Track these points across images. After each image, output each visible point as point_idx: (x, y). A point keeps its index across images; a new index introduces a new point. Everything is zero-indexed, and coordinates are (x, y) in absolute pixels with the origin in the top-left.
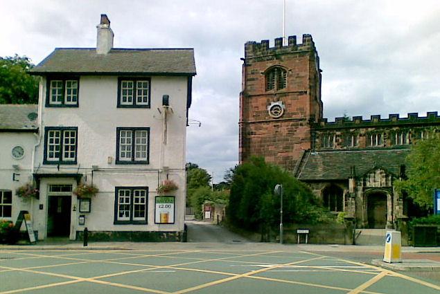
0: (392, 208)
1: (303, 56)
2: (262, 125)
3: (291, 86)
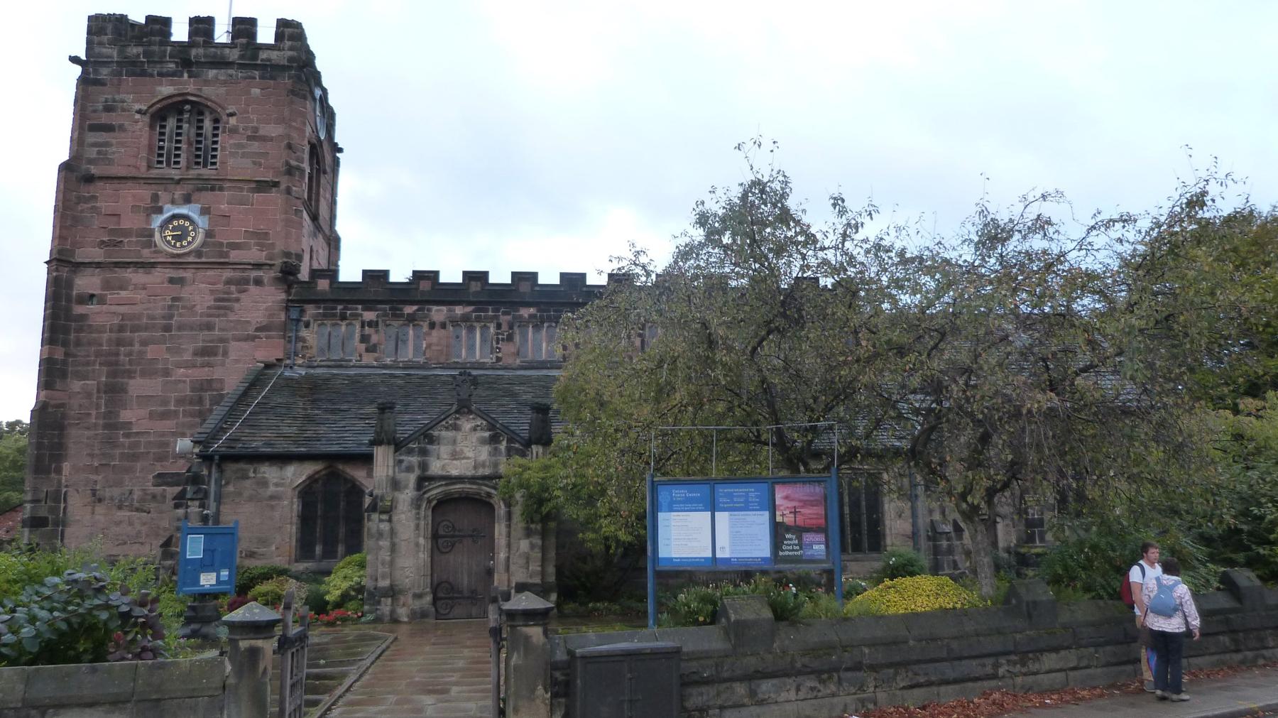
0: (509, 546)
1: (272, 78)
2: (129, 274)
3: (231, 162)
